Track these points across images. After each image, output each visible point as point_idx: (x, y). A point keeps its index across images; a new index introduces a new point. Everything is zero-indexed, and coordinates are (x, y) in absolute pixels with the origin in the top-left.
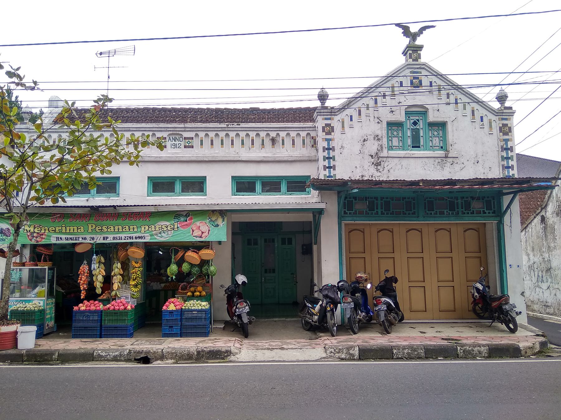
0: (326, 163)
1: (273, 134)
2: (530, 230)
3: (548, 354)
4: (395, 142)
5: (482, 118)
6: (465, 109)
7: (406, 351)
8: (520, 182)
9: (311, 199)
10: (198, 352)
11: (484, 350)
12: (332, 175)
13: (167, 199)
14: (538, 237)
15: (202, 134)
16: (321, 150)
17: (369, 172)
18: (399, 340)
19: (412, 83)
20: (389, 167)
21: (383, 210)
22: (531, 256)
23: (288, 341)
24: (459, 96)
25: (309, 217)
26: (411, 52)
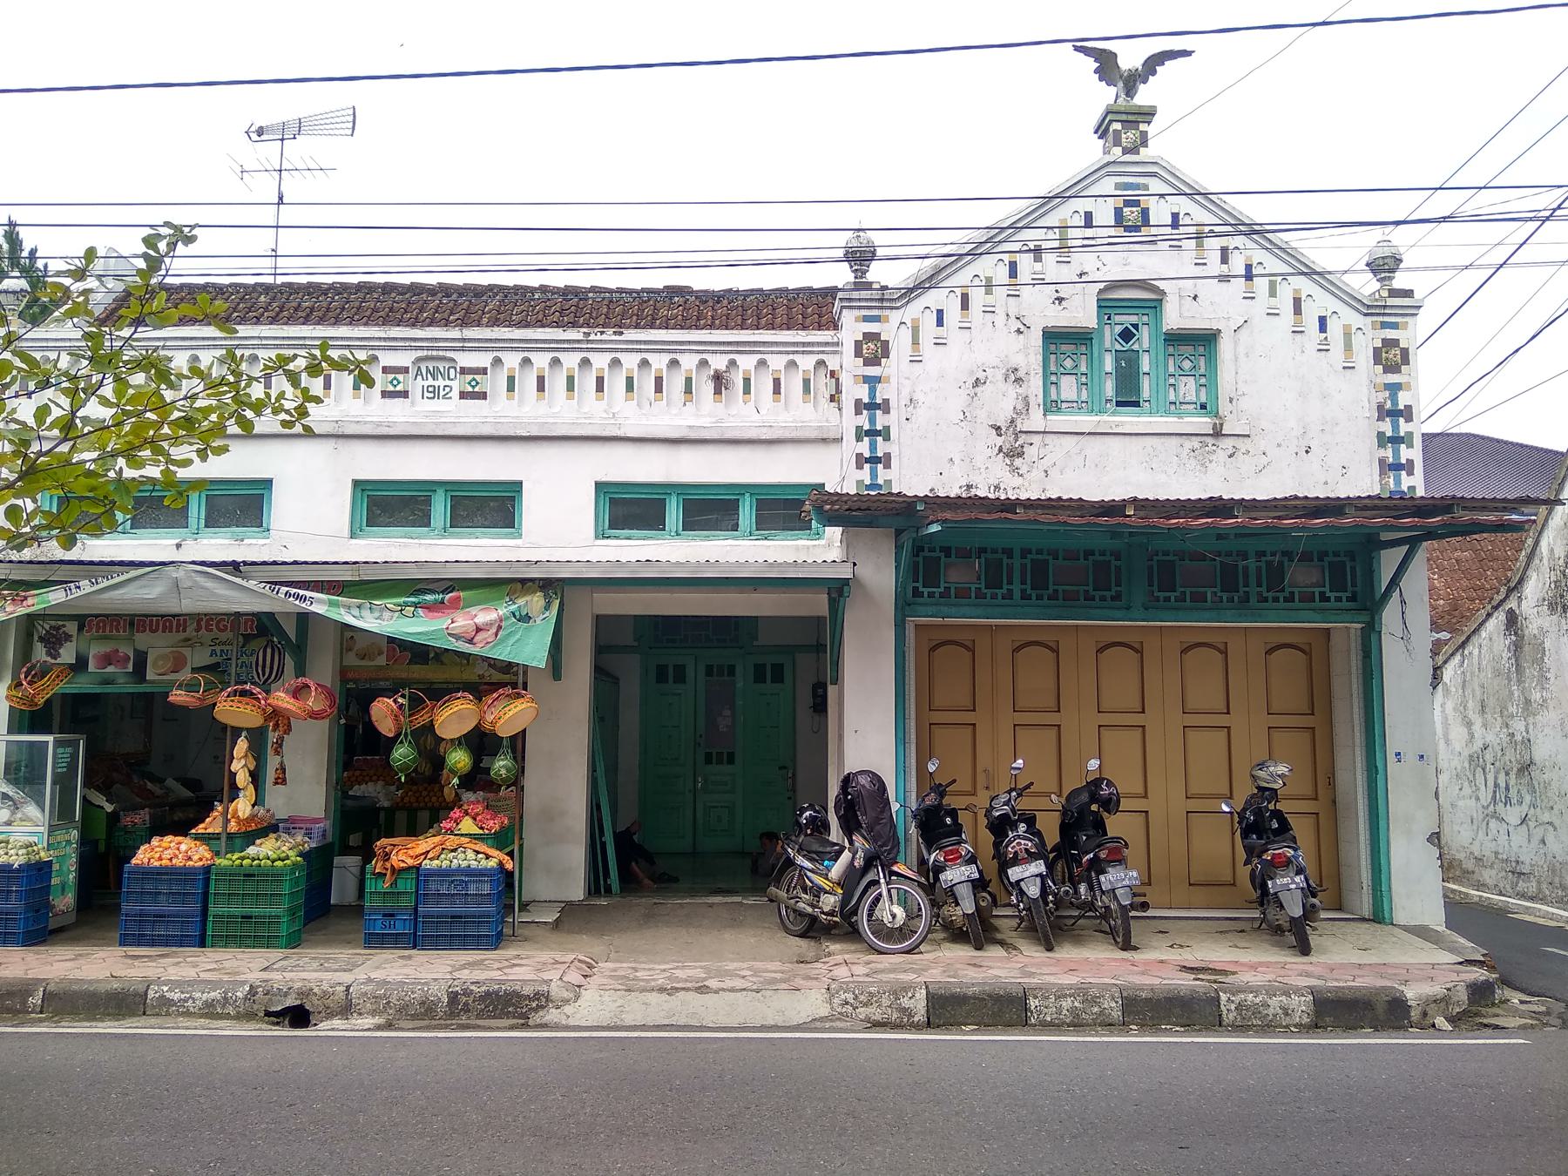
0: (864, 448)
1: (718, 362)
2: (1476, 652)
3: (1485, 1021)
4: (1068, 388)
5: (1323, 322)
6: (1273, 293)
7: (1066, 1004)
8: (1423, 508)
9: (821, 550)
10: (453, 997)
11: (1301, 1006)
12: (880, 481)
13: (406, 545)
14: (1497, 673)
15: (512, 360)
16: (848, 406)
17: (990, 477)
18: (1054, 969)
19: (1118, 213)
20: (1046, 463)
21: (1028, 587)
22: (1477, 727)
23: (732, 966)
24: (1258, 255)
25: (818, 605)
26: (1117, 126)
